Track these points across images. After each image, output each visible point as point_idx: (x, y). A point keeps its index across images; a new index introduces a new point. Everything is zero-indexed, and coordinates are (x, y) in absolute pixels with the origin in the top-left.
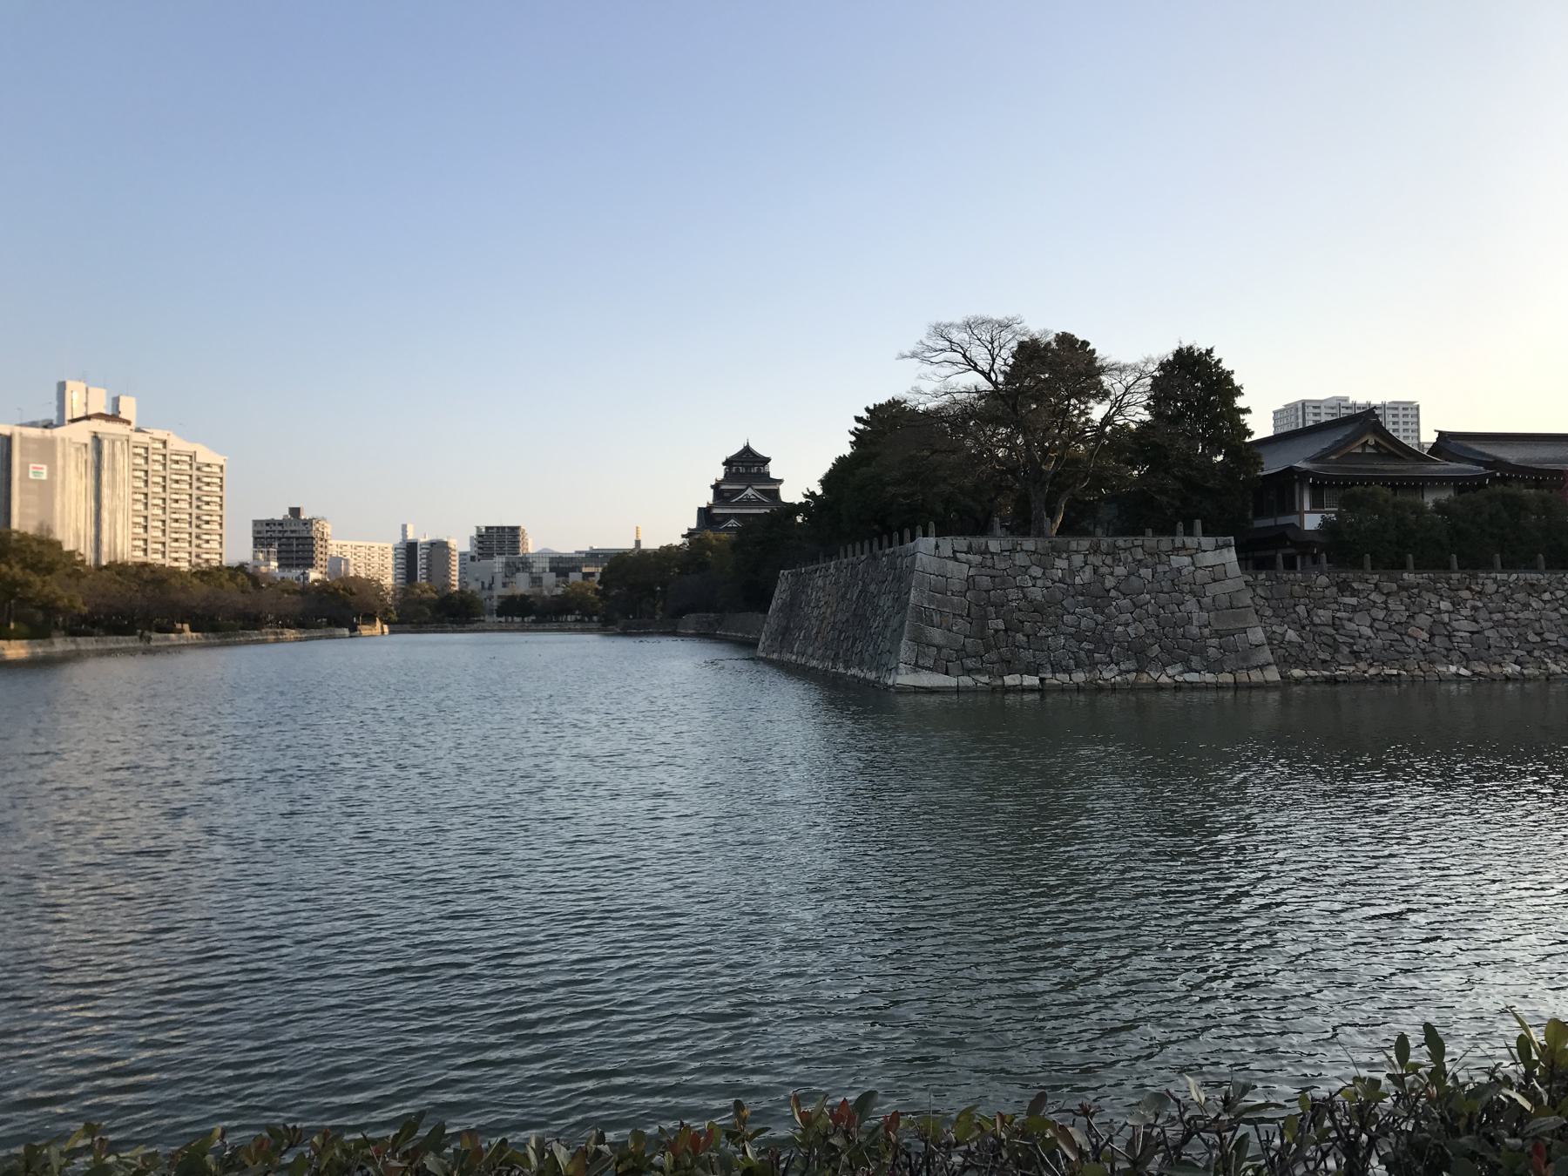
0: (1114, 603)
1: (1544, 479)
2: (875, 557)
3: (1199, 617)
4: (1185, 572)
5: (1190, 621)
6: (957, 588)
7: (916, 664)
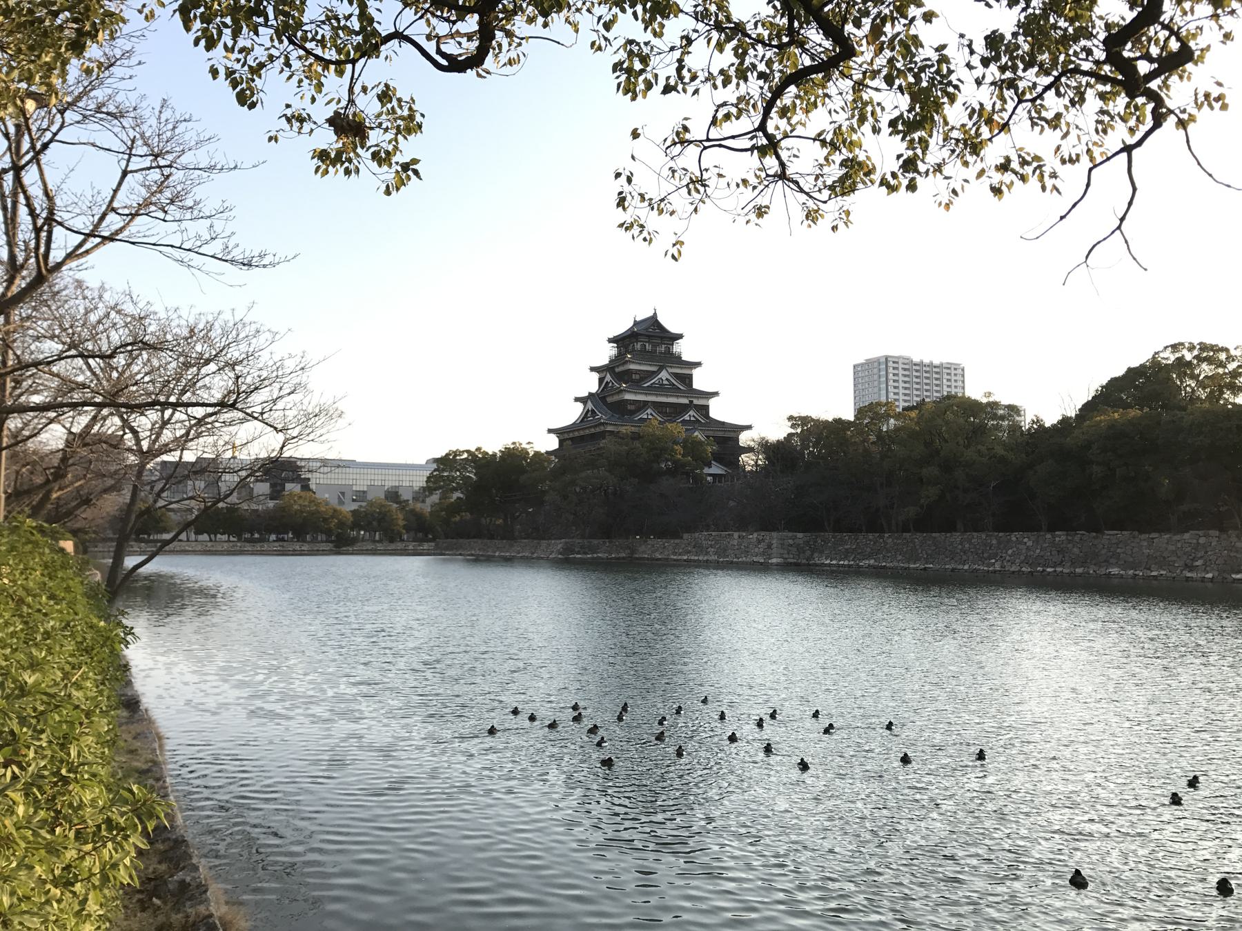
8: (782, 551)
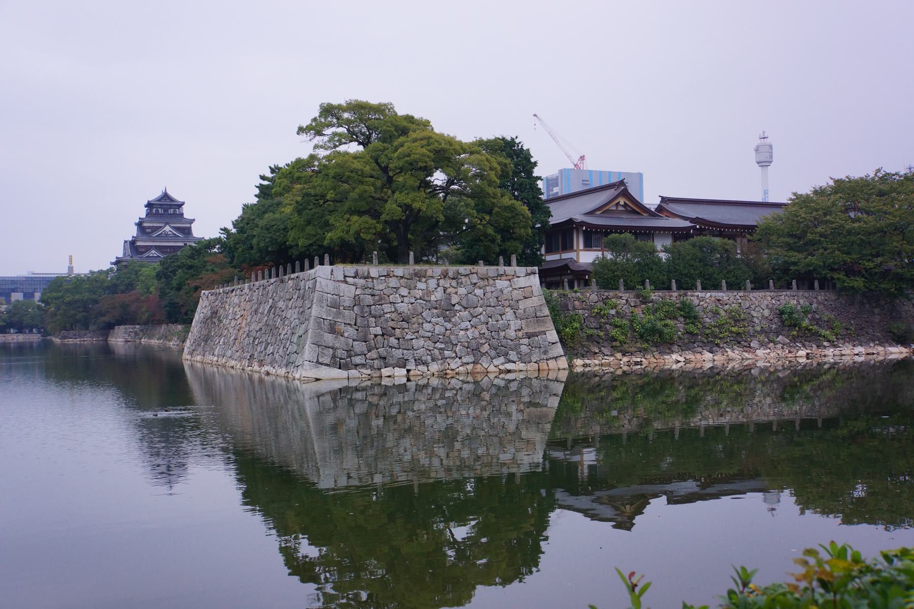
0: (458, 314)
1: (724, 231)
2: (282, 281)
3: (515, 324)
4: (505, 292)
5: (508, 326)
6: (347, 304)
7: (318, 362)
8: (124, 335)
